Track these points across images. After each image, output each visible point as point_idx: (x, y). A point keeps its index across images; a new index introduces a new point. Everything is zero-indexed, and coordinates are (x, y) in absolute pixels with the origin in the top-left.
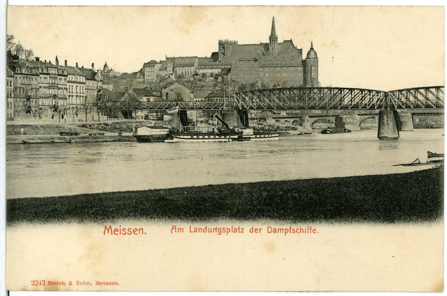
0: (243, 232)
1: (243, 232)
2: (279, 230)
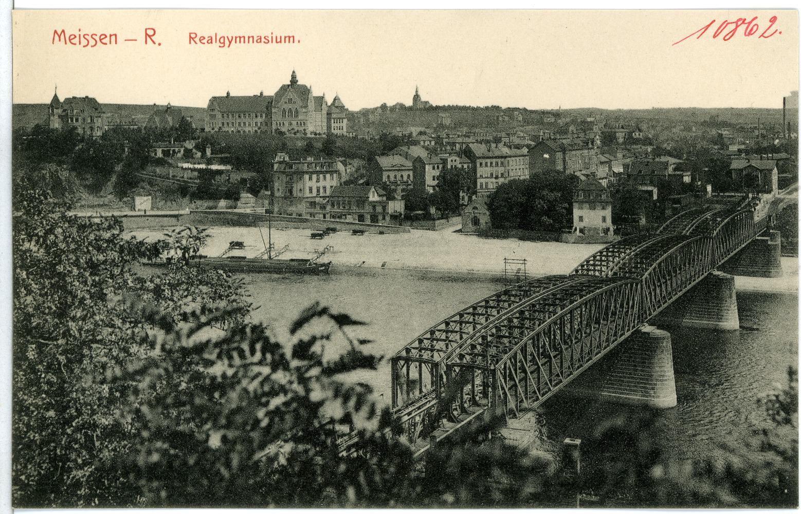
0: (190, 43)
1: (190, 43)
2: (287, 39)
